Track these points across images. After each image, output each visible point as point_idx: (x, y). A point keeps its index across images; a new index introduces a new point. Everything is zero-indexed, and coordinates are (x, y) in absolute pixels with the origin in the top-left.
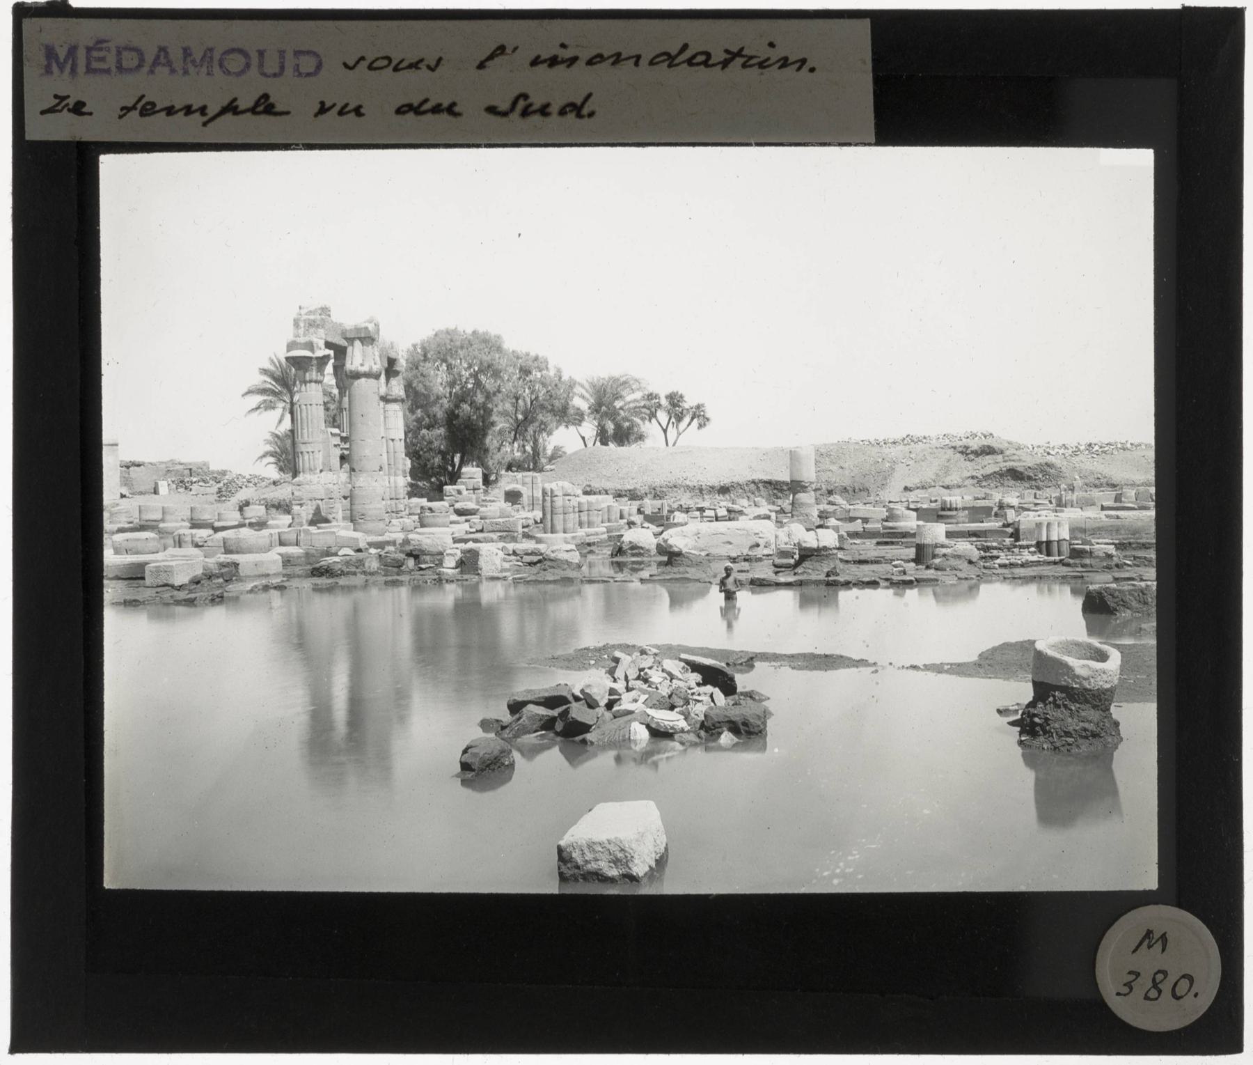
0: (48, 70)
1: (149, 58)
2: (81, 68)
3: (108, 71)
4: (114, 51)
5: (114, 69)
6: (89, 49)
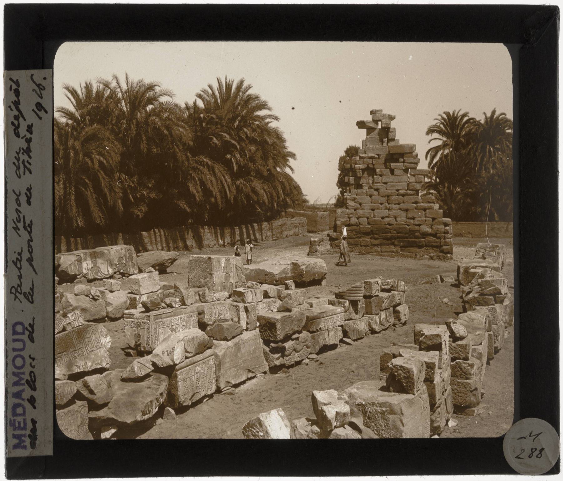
1: (17, 401)
3: (25, 420)
4: (15, 418)
5: (24, 417)
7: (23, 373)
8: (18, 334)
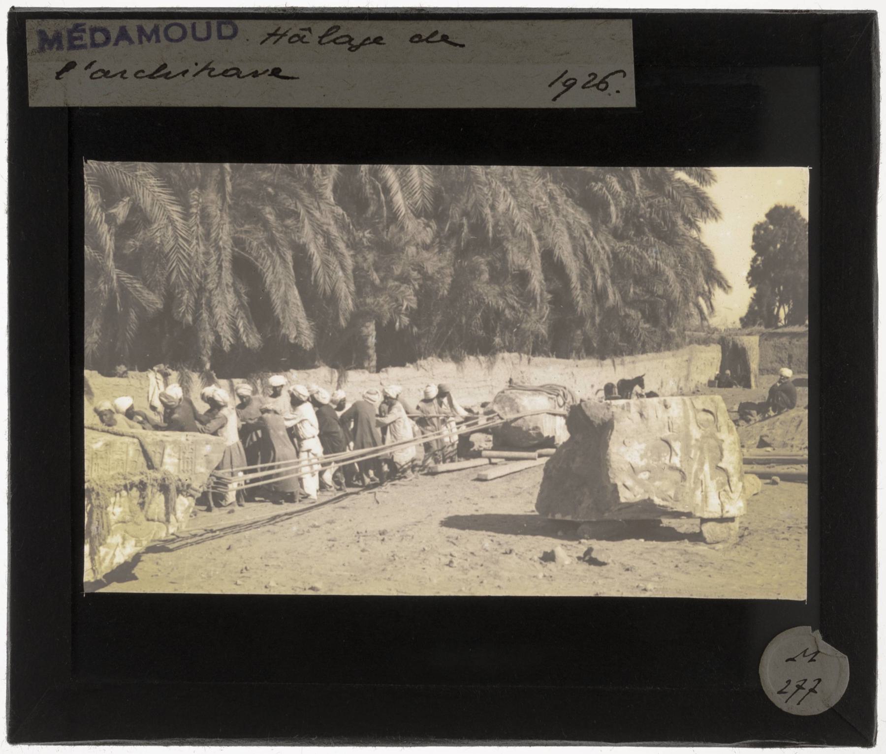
0: (42, 49)
2: (65, 43)
4: (88, 31)
5: (89, 44)
6: (70, 32)
7: (158, 41)
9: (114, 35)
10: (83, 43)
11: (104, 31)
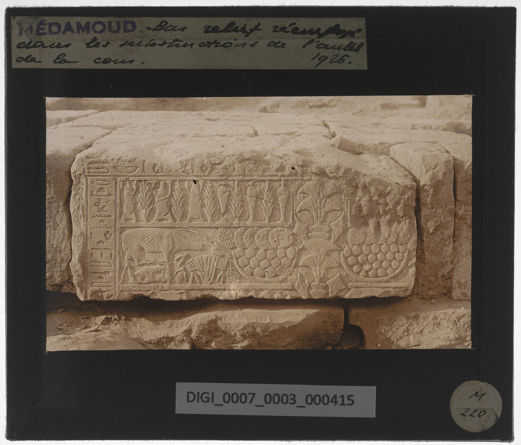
3: (45, 34)
4: (47, 25)
5: (48, 33)
8: (125, 27)
9: (63, 29)
10: (45, 31)
11: (58, 25)
